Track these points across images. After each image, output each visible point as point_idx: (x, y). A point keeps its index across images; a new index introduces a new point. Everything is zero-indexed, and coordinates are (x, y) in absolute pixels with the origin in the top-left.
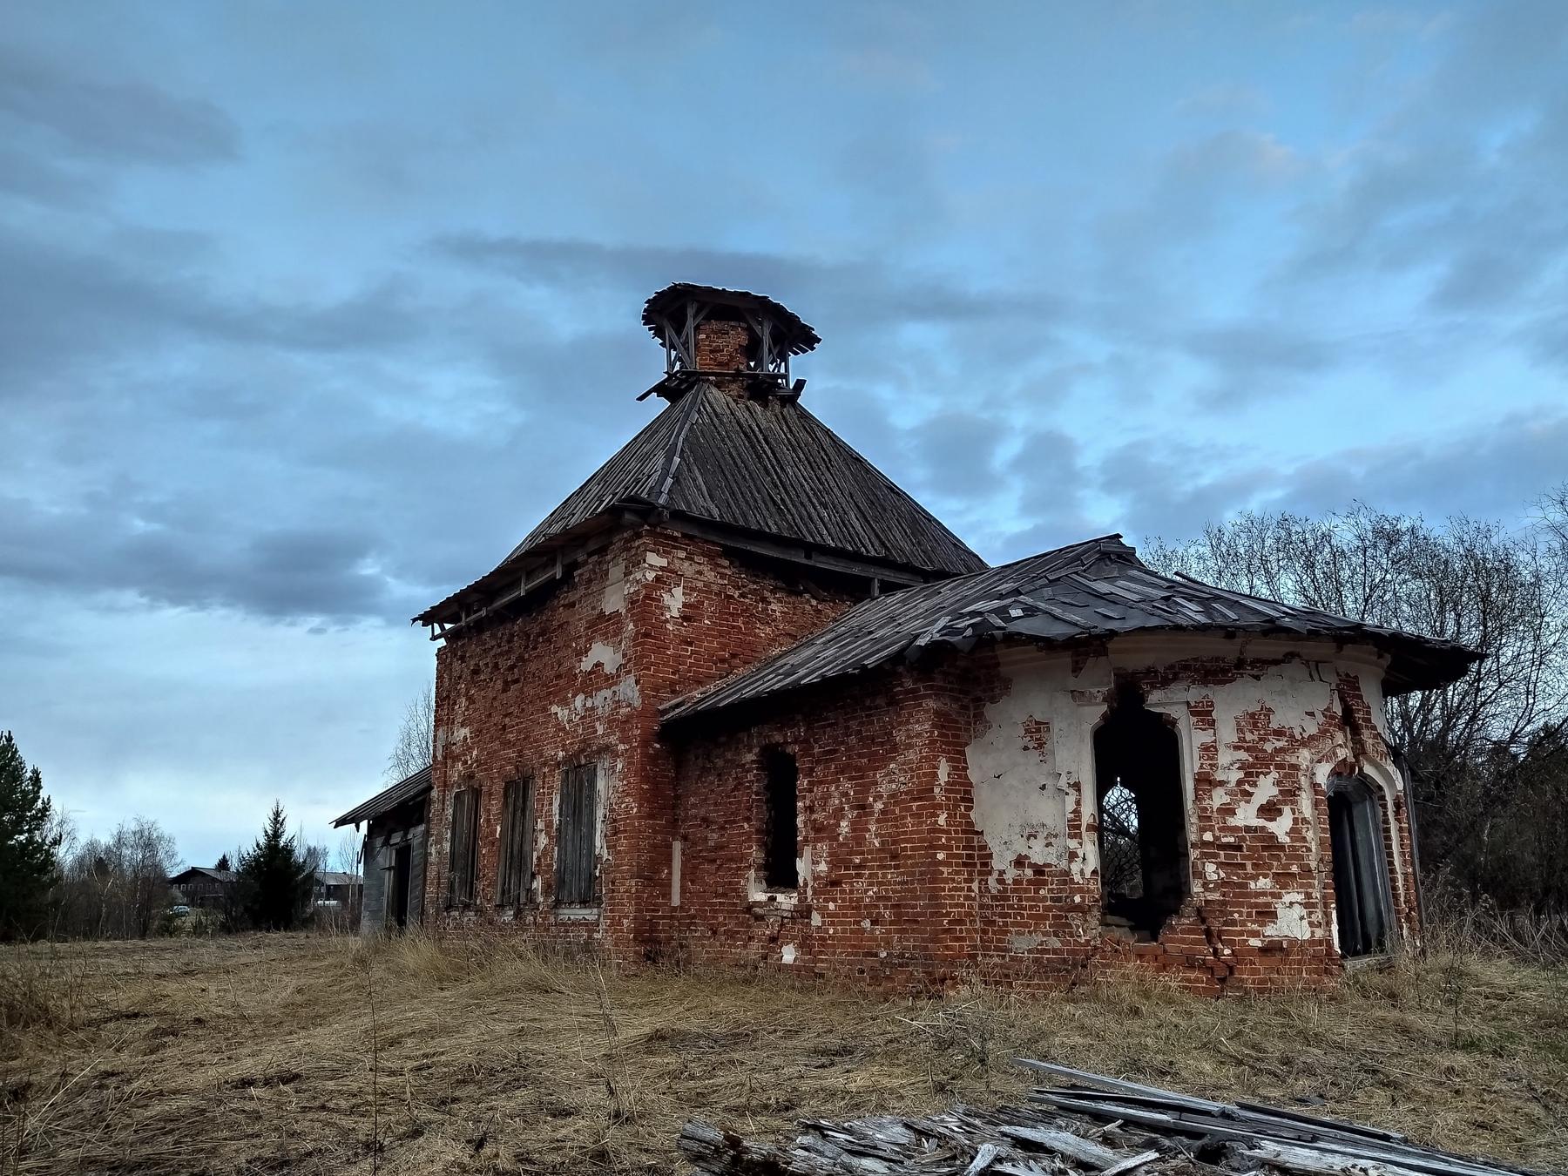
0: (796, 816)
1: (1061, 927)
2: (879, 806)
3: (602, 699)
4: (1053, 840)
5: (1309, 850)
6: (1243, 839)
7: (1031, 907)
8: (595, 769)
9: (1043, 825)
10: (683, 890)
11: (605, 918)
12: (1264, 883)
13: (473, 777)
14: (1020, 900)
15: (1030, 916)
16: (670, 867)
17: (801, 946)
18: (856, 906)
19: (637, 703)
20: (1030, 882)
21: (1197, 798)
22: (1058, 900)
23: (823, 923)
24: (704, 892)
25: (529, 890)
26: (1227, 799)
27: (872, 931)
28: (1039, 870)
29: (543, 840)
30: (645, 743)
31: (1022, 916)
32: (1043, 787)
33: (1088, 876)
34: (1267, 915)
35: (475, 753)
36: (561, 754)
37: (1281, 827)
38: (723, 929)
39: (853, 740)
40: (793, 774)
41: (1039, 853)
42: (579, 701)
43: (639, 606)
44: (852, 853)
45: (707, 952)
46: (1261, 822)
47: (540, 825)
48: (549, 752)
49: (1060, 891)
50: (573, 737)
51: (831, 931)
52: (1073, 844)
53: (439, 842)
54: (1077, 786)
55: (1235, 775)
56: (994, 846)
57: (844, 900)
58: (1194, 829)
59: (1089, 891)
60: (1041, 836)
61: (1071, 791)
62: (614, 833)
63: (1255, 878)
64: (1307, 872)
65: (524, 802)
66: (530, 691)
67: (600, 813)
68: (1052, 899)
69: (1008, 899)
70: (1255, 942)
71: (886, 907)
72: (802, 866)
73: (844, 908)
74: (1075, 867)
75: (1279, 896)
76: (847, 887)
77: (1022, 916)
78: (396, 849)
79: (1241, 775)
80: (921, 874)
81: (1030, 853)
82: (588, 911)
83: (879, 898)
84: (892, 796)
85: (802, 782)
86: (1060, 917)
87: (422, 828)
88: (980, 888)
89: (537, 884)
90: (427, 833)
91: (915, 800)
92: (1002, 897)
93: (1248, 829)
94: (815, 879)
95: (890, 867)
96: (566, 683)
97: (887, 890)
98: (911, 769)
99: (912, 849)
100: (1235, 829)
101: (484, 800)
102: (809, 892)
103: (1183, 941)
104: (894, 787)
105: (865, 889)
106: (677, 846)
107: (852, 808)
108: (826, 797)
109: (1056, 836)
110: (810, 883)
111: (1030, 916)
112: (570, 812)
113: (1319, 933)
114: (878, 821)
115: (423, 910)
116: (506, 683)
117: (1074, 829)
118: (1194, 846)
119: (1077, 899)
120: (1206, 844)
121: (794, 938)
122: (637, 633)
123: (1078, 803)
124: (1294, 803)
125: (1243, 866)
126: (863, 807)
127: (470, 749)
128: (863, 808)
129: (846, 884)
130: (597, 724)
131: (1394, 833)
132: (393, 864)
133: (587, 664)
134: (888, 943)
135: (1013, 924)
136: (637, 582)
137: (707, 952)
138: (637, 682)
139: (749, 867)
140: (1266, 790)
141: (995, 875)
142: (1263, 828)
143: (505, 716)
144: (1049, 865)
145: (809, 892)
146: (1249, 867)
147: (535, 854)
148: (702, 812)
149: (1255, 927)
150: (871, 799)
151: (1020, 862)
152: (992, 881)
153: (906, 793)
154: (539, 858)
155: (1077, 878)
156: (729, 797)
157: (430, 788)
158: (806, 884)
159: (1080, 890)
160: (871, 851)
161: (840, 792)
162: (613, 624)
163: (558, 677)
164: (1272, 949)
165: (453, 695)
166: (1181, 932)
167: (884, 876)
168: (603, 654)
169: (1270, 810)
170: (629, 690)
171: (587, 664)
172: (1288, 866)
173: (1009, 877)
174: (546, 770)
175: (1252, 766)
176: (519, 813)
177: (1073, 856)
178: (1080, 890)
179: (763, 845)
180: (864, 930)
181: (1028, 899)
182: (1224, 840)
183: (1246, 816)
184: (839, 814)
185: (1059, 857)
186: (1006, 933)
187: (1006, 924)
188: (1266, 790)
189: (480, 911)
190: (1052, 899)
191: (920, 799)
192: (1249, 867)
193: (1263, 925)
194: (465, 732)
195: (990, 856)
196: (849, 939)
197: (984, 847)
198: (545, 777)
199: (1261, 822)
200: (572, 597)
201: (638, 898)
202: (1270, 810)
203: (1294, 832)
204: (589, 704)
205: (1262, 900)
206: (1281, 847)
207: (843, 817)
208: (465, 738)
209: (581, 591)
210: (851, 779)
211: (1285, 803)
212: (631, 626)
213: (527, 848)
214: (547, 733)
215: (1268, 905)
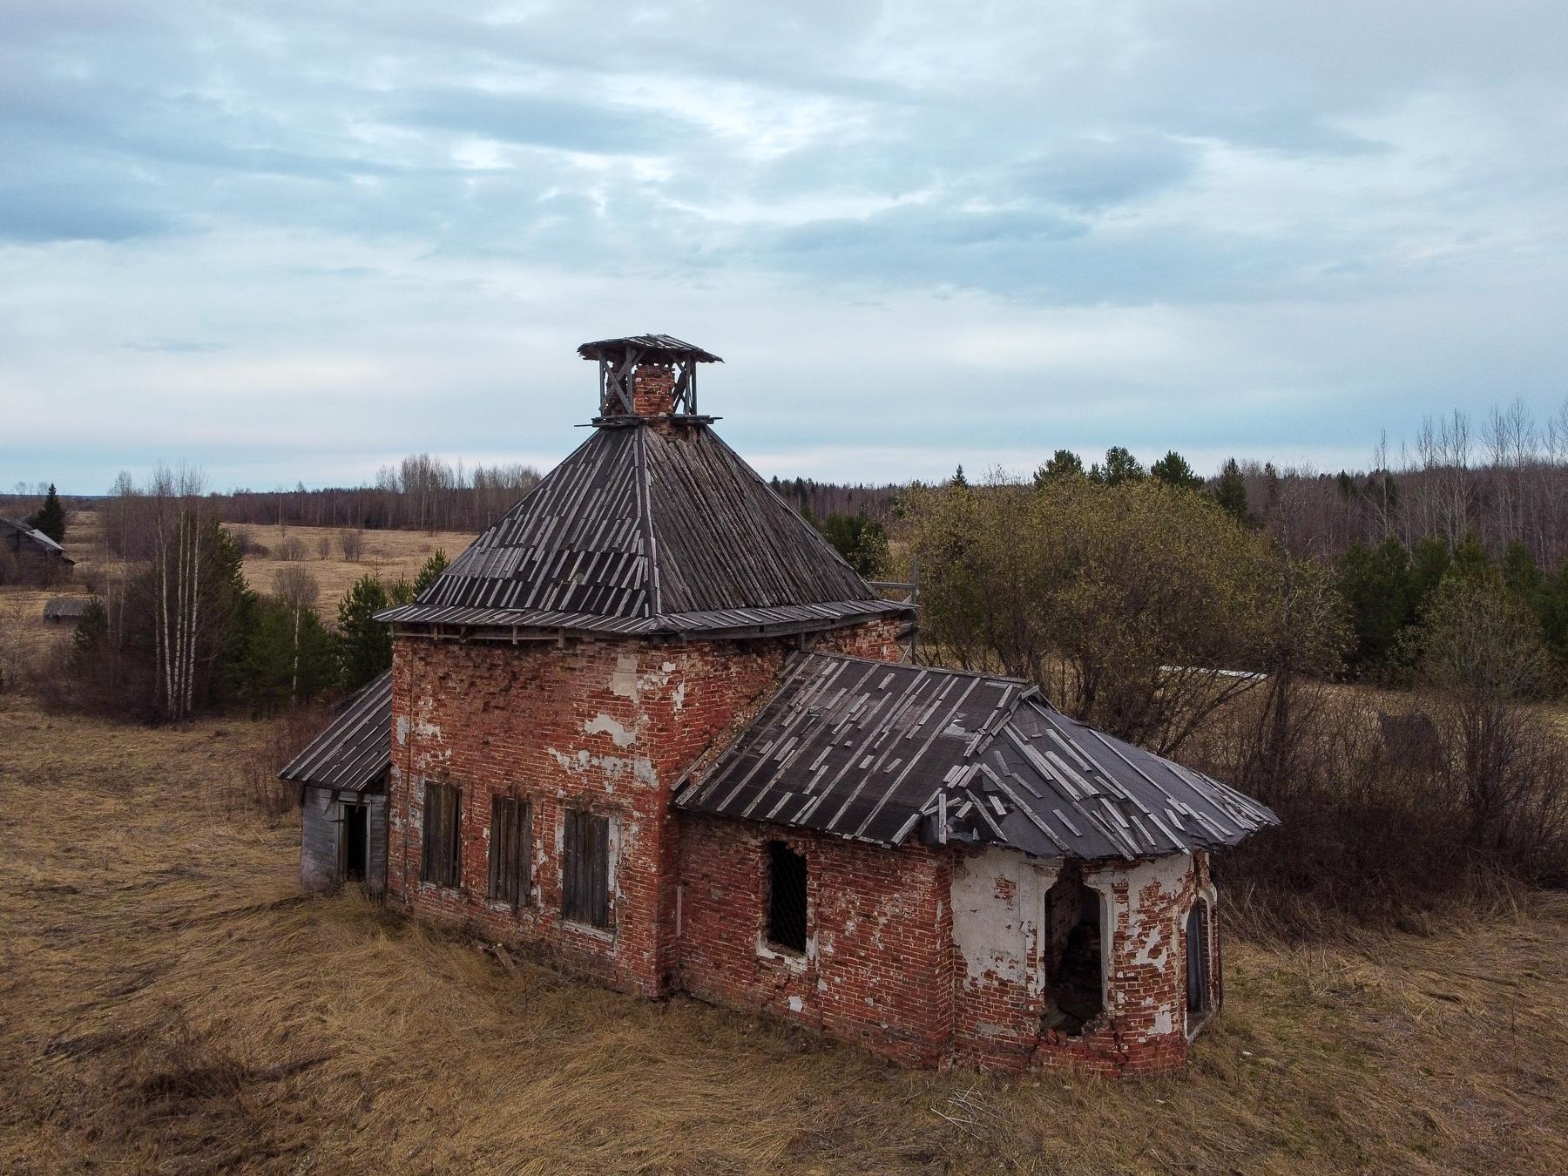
0: (805, 909)
1: (1017, 1025)
2: (883, 920)
4: (1015, 965)
5: (1174, 973)
6: (1139, 973)
7: (996, 1007)
8: (607, 819)
9: (1008, 953)
10: (685, 925)
11: (619, 942)
12: (1149, 1001)
13: (448, 774)
14: (988, 1000)
15: (995, 1013)
16: (675, 908)
17: (807, 1000)
18: (862, 986)
19: (655, 784)
20: (996, 990)
21: (1115, 949)
22: (1017, 1005)
23: (830, 990)
24: (707, 931)
25: (528, 896)
26: (1131, 947)
27: (875, 1007)
28: (1003, 983)
29: (542, 858)
30: (661, 817)
31: (989, 1011)
32: (1009, 927)
33: (1039, 993)
34: (1150, 1021)
35: (449, 753)
36: (561, 792)
37: (1159, 963)
38: (727, 966)
39: (859, 865)
40: (802, 875)
41: (1003, 972)
42: (583, 755)
43: (655, 704)
44: (857, 946)
45: (710, 979)
46: (1150, 961)
47: (539, 844)
48: (546, 785)
49: (1018, 999)
50: (575, 783)
51: (837, 998)
52: (1030, 971)
53: (404, 814)
54: (1035, 932)
55: (1138, 930)
56: (969, 958)
57: (849, 978)
58: (1111, 968)
59: (1038, 1002)
60: (1007, 960)
61: (1030, 935)
62: (627, 876)
63: (1144, 998)
64: (1172, 988)
65: (521, 819)
67: (613, 859)
68: (1012, 1004)
69: (978, 997)
70: (1142, 1040)
71: (888, 994)
72: (811, 945)
73: (850, 984)
74: (1031, 987)
75: (1156, 1008)
76: (853, 971)
77: (989, 1011)
78: (346, 806)
79: (1140, 930)
80: (921, 980)
81: (998, 970)
82: (599, 932)
83: (880, 986)
84: (892, 916)
85: (812, 883)
86: (1018, 1017)
87: (384, 799)
88: (955, 985)
89: (536, 892)
90: (388, 805)
91: (917, 927)
92: (974, 994)
93: (1142, 966)
94: (821, 955)
95: (892, 967)
96: (567, 737)
97: (889, 983)
98: (915, 905)
99: (913, 961)
100: (1136, 967)
101: (465, 801)
102: (817, 965)
103: (1100, 1041)
104: (897, 911)
106: (679, 889)
107: (858, 914)
108: (833, 901)
109: (1017, 962)
110: (818, 958)
111: (995, 1013)
112: (581, 850)
113: (1177, 1027)
114: (881, 930)
115: (387, 870)
116: (486, 704)
117: (1031, 961)
118: (1110, 979)
119: (1031, 1008)
120: (1118, 979)
121: (800, 993)
122: (653, 726)
123: (1035, 944)
124: (1168, 943)
125: (1138, 991)
126: (868, 917)
127: (443, 748)
129: (851, 967)
130: (606, 783)
131: (1210, 931)
132: (342, 817)
134: (890, 1020)
135: (981, 1015)
136: (653, 683)
137: (710, 979)
138: (654, 766)
139: (756, 929)
140: (1154, 938)
141: (970, 979)
142: (1151, 965)
143: (488, 734)
144: (1012, 982)
145: (817, 965)
146: (1142, 991)
147: (534, 868)
148: (704, 870)
149: (1143, 1030)
150: (876, 913)
151: (989, 974)
152: (966, 983)
153: (910, 920)
154: (538, 871)
155: (1032, 994)
156: (732, 866)
157: (390, 765)
158: (815, 959)
159: (1034, 1002)
160: (873, 951)
161: (849, 899)
162: (622, 705)
164: (1152, 1042)
165: (416, 690)
166: (1100, 1037)
167: (887, 971)
169: (1155, 952)
170: (646, 771)
171: (594, 726)
172: (1162, 988)
173: (982, 982)
174: (544, 800)
175: (1147, 923)
176: (514, 829)
177: (1029, 979)
178: (1034, 1002)
179: (765, 910)
180: (868, 1005)
181: (994, 1001)
182: (1128, 975)
183: (1142, 958)
184: (845, 915)
185: (1019, 977)
186: (975, 1020)
187: (976, 1014)
188: (1154, 938)
189: (466, 893)
190: (1012, 1004)
191: (922, 928)
192: (1142, 991)
193: (1147, 1028)
195: (966, 965)
196: (854, 1007)
197: (961, 958)
198: (543, 805)
199: (1150, 961)
200: (570, 662)
201: (658, 938)
202: (1155, 952)
203: (1168, 965)
204: (595, 762)
205: (1147, 1012)
206: (1159, 975)
207: (849, 918)
208: (434, 736)
209: (583, 663)
210: (858, 892)
211: (1162, 945)
212: (646, 717)
213: (524, 860)
214: (543, 768)
215: (1151, 1015)
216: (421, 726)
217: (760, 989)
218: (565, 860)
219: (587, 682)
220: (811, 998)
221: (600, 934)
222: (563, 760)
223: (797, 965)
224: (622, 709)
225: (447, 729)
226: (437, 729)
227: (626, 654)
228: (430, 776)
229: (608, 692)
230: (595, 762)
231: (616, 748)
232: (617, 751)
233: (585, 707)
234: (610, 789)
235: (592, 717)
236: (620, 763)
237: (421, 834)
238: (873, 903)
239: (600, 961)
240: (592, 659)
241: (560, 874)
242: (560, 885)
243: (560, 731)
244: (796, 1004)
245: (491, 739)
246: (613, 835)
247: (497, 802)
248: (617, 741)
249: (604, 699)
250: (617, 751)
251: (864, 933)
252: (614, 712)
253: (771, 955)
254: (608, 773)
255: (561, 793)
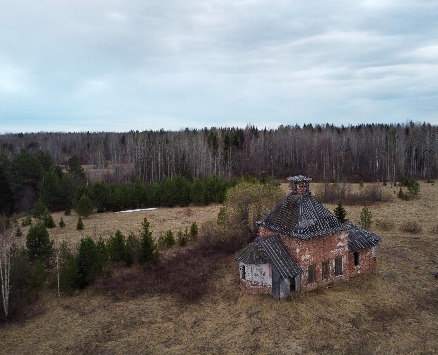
3: (341, 250)
18: (365, 266)
29: (331, 269)
35: (312, 259)
39: (365, 251)
42: (337, 250)
48: (330, 257)
66: (326, 248)
67: (342, 263)
96: (334, 248)
101: (317, 266)
105: (366, 264)
127: (312, 258)
128: (366, 257)
133: (338, 245)
163: (332, 246)
168: (340, 244)
171: (338, 245)
184: (363, 258)
194: (308, 256)
204: (339, 250)
209: (336, 235)
216: (306, 256)
217: (355, 272)
218: (335, 267)
219: (337, 238)
220: (360, 271)
221: (340, 276)
222: (333, 252)
223: (359, 267)
224: (342, 240)
225: (312, 255)
226: (310, 256)
227: (343, 232)
228: (309, 264)
229: (340, 238)
230: (339, 250)
231: (341, 247)
232: (342, 247)
233: (337, 242)
234: (341, 253)
235: (338, 243)
236: (342, 249)
237: (308, 276)
238: (366, 255)
239: (341, 280)
240: (337, 234)
241: (334, 270)
242: (334, 272)
243: (333, 247)
244: (359, 272)
245: (320, 253)
246: (343, 260)
247: (323, 264)
248: (342, 246)
249: (340, 240)
250: (342, 247)
251: (365, 259)
252: (341, 241)
253: (356, 267)
254: (341, 251)
255: (333, 257)
